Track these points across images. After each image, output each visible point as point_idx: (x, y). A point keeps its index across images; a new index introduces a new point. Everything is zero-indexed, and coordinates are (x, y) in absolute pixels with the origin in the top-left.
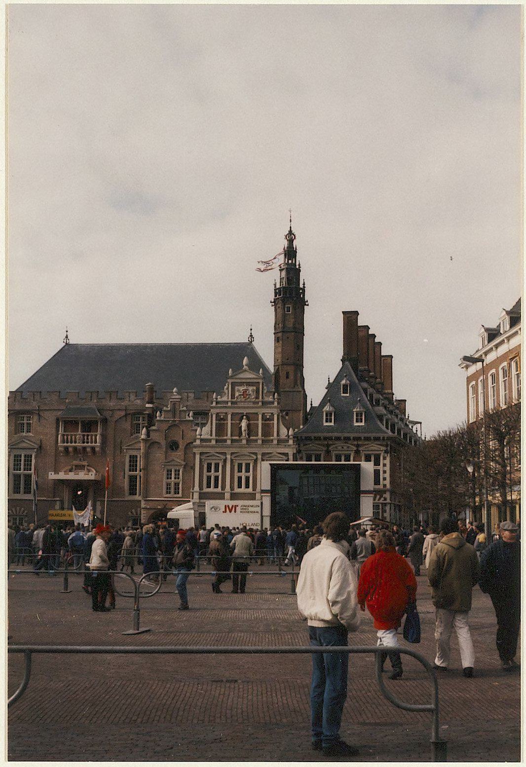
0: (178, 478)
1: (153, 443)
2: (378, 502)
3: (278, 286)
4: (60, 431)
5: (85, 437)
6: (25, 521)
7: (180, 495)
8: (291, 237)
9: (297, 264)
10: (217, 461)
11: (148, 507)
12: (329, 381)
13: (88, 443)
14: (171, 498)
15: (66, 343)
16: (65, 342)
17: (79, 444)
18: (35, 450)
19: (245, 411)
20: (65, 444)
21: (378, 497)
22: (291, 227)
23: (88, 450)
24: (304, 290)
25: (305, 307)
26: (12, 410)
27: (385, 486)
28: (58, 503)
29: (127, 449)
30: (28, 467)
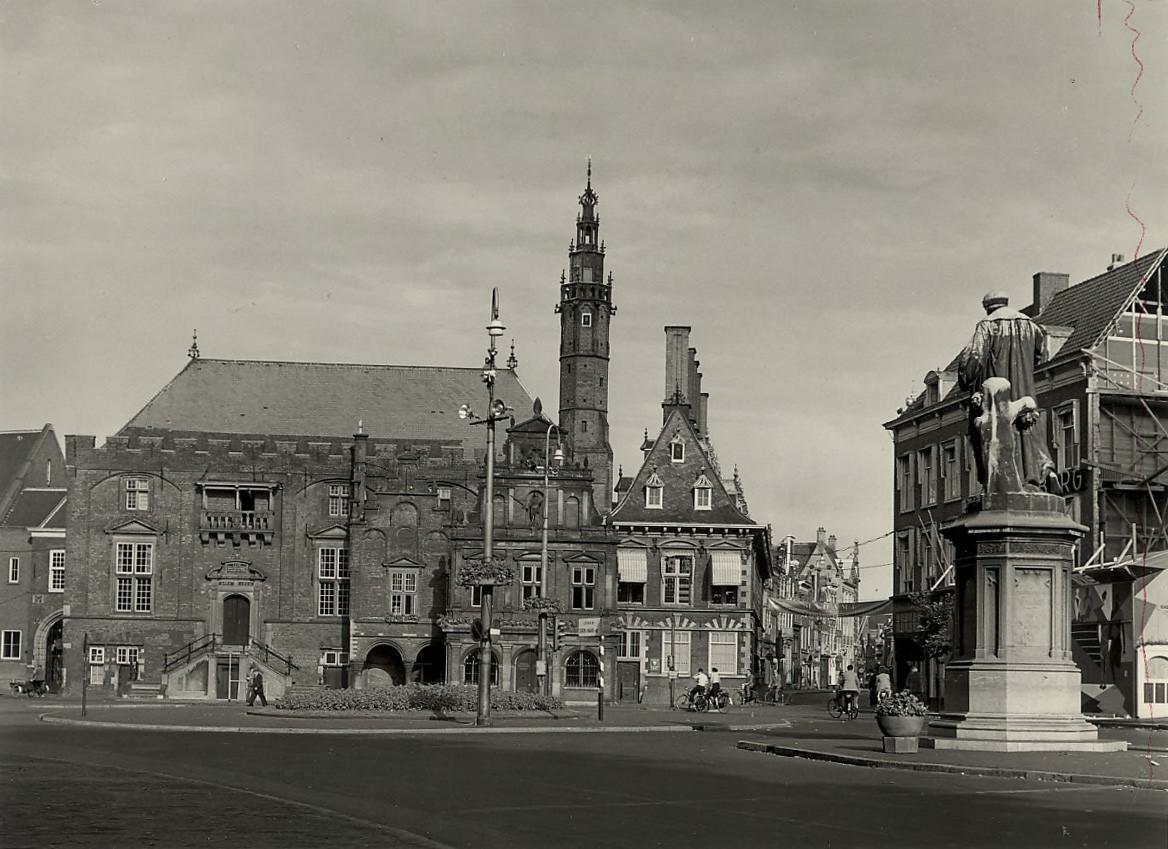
3: (567, 282)
8: (589, 199)
9: (599, 245)
11: (362, 634)
15: (194, 357)
21: (733, 621)
22: (589, 183)
24: (609, 287)
25: (611, 316)
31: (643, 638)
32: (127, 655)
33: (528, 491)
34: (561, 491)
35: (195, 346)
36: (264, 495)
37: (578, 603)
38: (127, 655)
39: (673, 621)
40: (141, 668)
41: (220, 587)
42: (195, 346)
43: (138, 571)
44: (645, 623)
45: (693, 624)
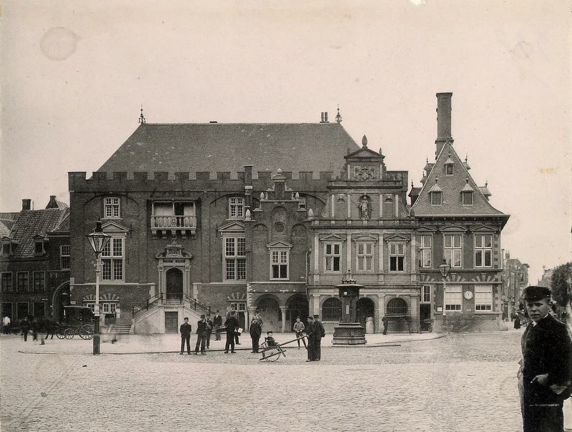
0: (285, 261)
1: (258, 225)
2: (490, 283)
4: (153, 213)
5: (180, 220)
6: (118, 308)
7: (288, 279)
10: (337, 243)
11: (254, 291)
12: (427, 162)
13: (183, 225)
14: (277, 281)
15: (142, 123)
16: (141, 121)
17: (175, 228)
18: (126, 234)
19: (365, 192)
20: (158, 227)
23: (183, 232)
26: (99, 192)
27: (496, 266)
28: (153, 289)
29: (223, 232)
30: (117, 251)
31: (432, 290)
32: (110, 308)
33: (361, 195)
34: (381, 195)
35: (142, 116)
36: (190, 205)
37: (393, 268)
38: (110, 308)
39: (451, 278)
40: (118, 316)
41: (166, 264)
42: (142, 116)
43: (114, 255)
44: (433, 280)
45: (464, 279)
